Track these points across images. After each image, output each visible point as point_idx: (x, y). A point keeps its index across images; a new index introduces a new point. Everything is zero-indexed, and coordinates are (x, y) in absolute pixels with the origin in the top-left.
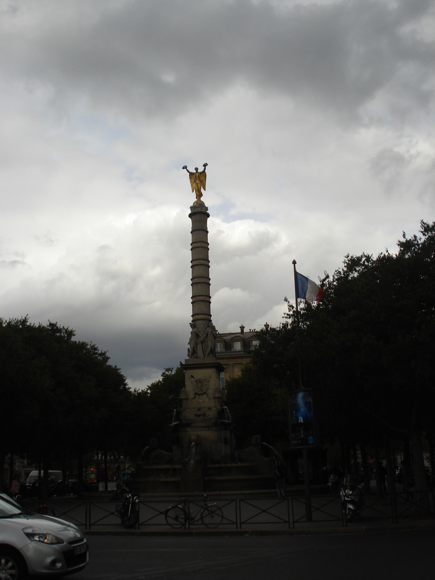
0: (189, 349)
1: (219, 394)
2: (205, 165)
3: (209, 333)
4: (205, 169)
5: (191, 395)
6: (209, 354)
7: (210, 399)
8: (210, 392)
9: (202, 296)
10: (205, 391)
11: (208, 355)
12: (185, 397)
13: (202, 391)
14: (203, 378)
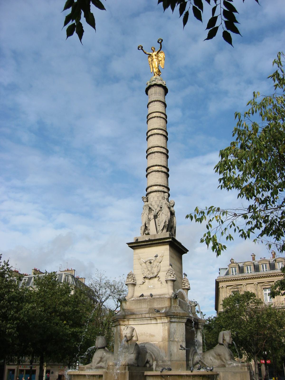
1: (172, 276)
5: (139, 280)
6: (163, 230)
8: (163, 276)
9: (156, 166)
10: (155, 274)
11: (163, 230)
12: (131, 282)
13: (153, 273)
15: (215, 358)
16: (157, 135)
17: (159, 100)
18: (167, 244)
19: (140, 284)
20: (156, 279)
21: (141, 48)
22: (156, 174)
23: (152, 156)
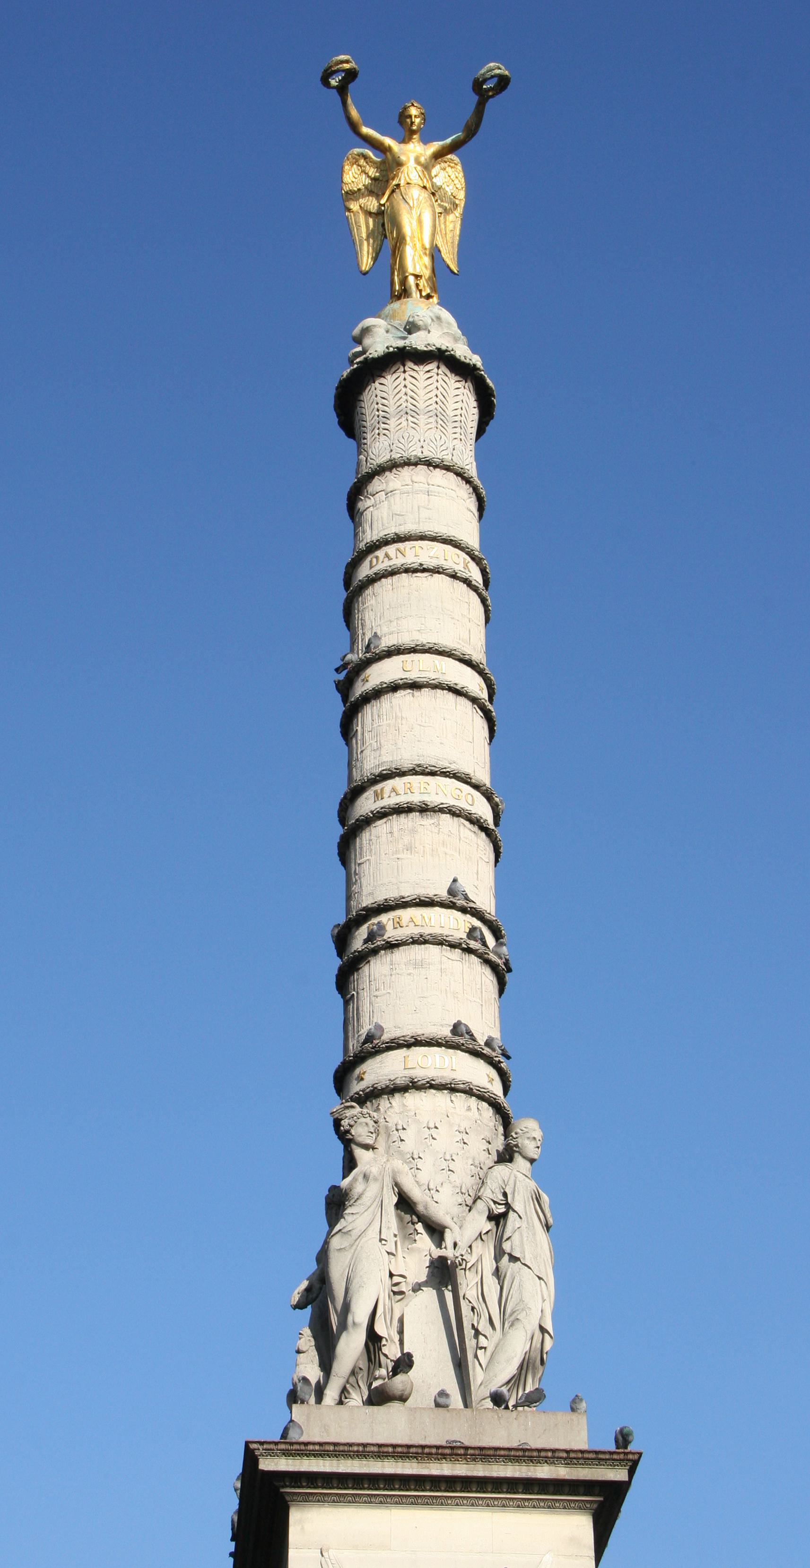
3: (517, 1205)
16: (451, 696)
18: (581, 1507)
23: (413, 831)
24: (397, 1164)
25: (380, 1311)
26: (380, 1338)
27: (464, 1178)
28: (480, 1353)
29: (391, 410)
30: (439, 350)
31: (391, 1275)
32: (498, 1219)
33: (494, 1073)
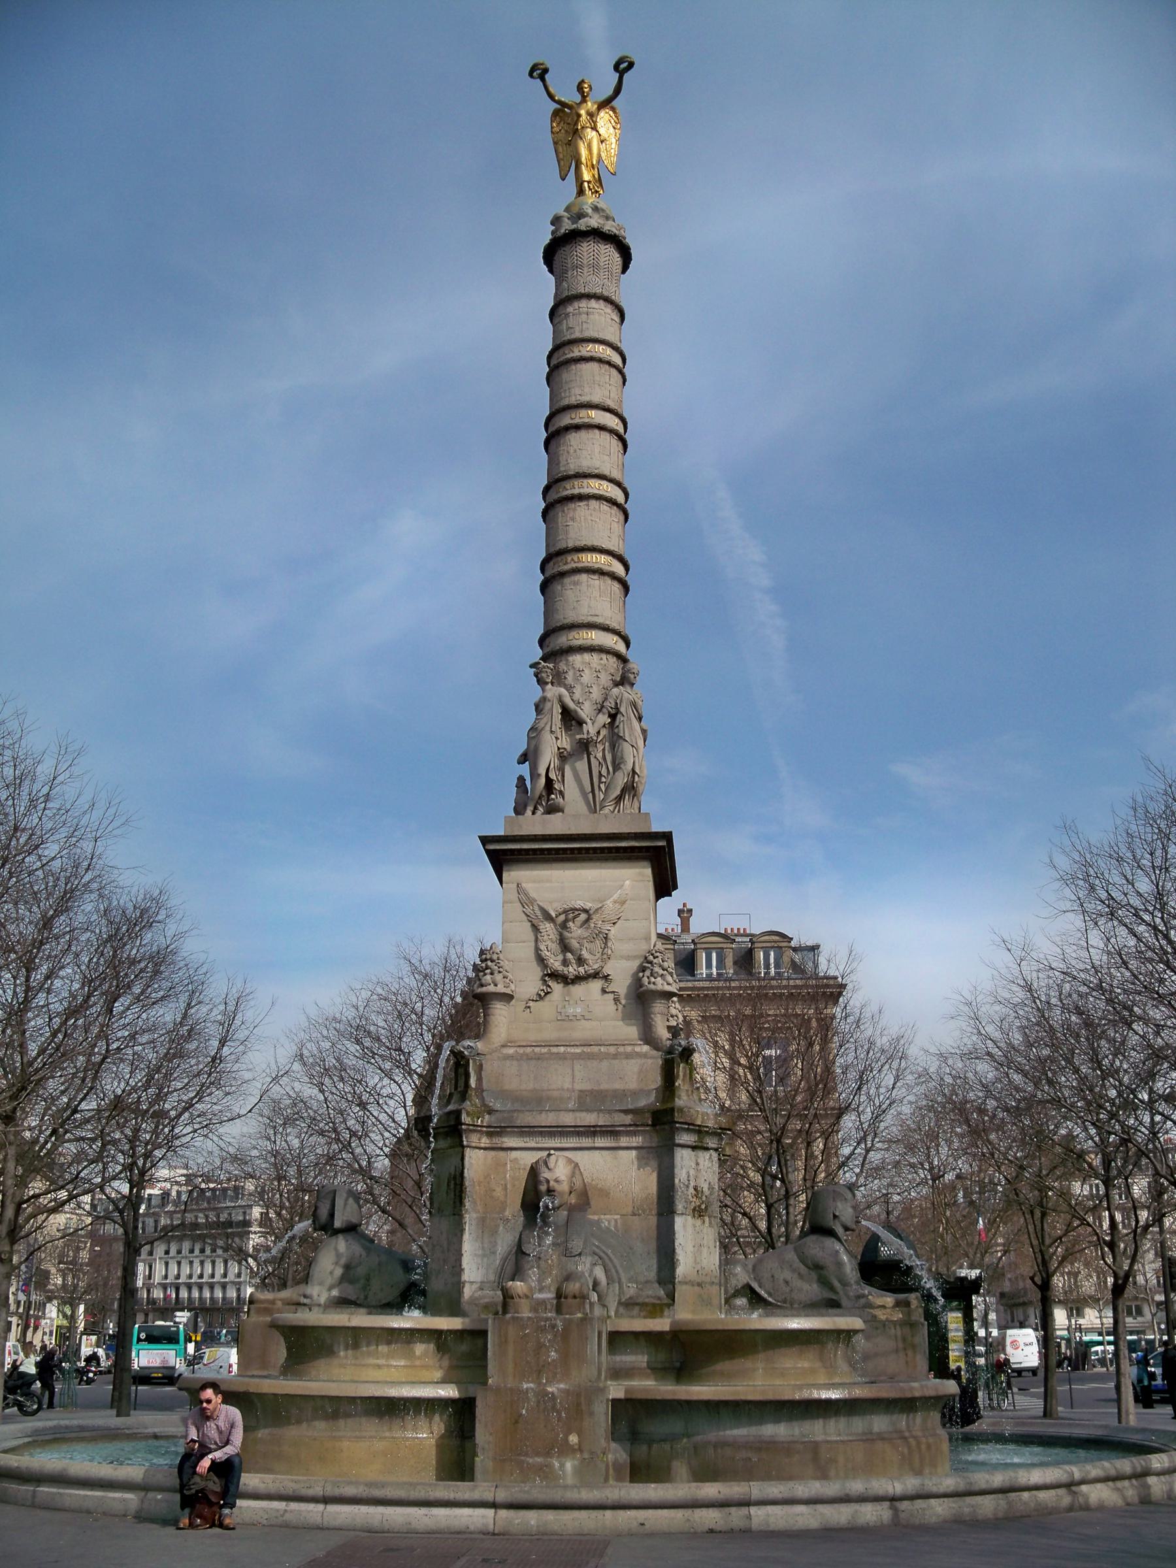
0: (521, 779)
1: (669, 979)
2: (623, 66)
3: (622, 710)
4: (618, 91)
6: (619, 799)
7: (616, 1000)
10: (593, 965)
12: (500, 989)
14: (588, 905)
15: (801, 1276)
16: (597, 431)
17: (606, 293)
18: (644, 859)
19: (528, 997)
20: (596, 985)
21: (539, 72)
22: (592, 582)
24: (563, 691)
25: (552, 766)
26: (552, 780)
27: (596, 694)
28: (602, 786)
29: (569, 266)
30: (594, 229)
31: (559, 749)
32: (613, 717)
33: (616, 638)
